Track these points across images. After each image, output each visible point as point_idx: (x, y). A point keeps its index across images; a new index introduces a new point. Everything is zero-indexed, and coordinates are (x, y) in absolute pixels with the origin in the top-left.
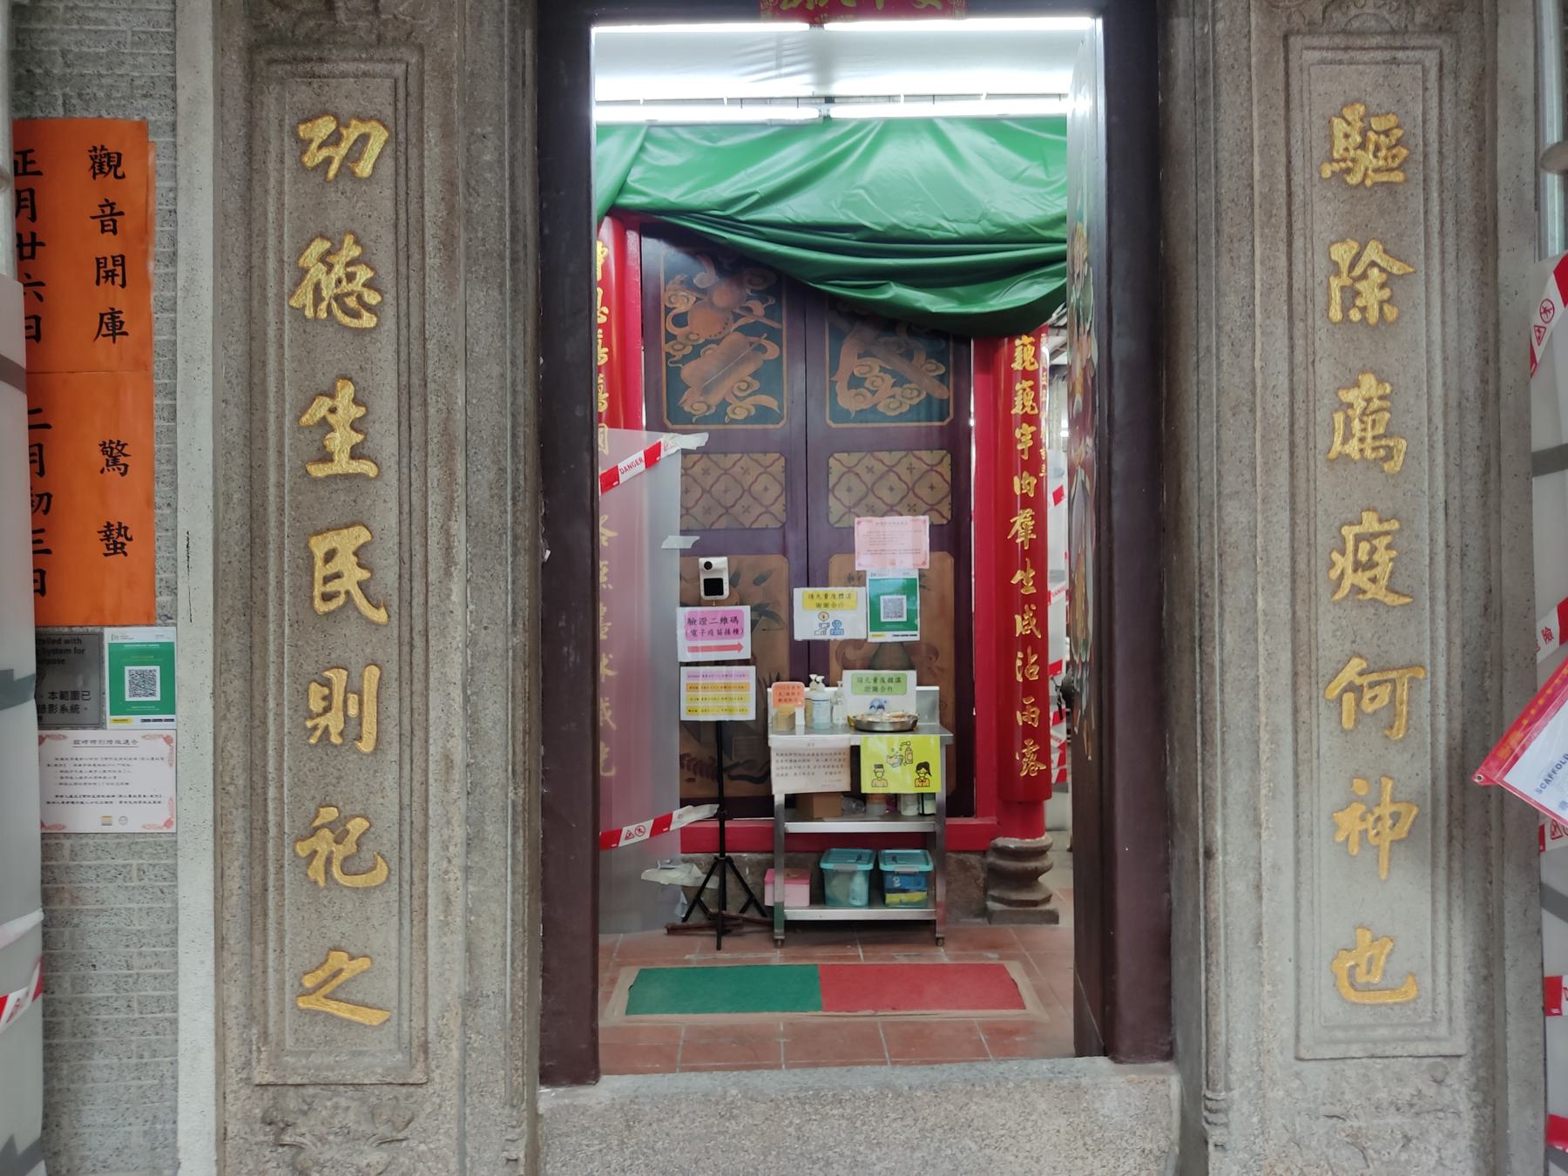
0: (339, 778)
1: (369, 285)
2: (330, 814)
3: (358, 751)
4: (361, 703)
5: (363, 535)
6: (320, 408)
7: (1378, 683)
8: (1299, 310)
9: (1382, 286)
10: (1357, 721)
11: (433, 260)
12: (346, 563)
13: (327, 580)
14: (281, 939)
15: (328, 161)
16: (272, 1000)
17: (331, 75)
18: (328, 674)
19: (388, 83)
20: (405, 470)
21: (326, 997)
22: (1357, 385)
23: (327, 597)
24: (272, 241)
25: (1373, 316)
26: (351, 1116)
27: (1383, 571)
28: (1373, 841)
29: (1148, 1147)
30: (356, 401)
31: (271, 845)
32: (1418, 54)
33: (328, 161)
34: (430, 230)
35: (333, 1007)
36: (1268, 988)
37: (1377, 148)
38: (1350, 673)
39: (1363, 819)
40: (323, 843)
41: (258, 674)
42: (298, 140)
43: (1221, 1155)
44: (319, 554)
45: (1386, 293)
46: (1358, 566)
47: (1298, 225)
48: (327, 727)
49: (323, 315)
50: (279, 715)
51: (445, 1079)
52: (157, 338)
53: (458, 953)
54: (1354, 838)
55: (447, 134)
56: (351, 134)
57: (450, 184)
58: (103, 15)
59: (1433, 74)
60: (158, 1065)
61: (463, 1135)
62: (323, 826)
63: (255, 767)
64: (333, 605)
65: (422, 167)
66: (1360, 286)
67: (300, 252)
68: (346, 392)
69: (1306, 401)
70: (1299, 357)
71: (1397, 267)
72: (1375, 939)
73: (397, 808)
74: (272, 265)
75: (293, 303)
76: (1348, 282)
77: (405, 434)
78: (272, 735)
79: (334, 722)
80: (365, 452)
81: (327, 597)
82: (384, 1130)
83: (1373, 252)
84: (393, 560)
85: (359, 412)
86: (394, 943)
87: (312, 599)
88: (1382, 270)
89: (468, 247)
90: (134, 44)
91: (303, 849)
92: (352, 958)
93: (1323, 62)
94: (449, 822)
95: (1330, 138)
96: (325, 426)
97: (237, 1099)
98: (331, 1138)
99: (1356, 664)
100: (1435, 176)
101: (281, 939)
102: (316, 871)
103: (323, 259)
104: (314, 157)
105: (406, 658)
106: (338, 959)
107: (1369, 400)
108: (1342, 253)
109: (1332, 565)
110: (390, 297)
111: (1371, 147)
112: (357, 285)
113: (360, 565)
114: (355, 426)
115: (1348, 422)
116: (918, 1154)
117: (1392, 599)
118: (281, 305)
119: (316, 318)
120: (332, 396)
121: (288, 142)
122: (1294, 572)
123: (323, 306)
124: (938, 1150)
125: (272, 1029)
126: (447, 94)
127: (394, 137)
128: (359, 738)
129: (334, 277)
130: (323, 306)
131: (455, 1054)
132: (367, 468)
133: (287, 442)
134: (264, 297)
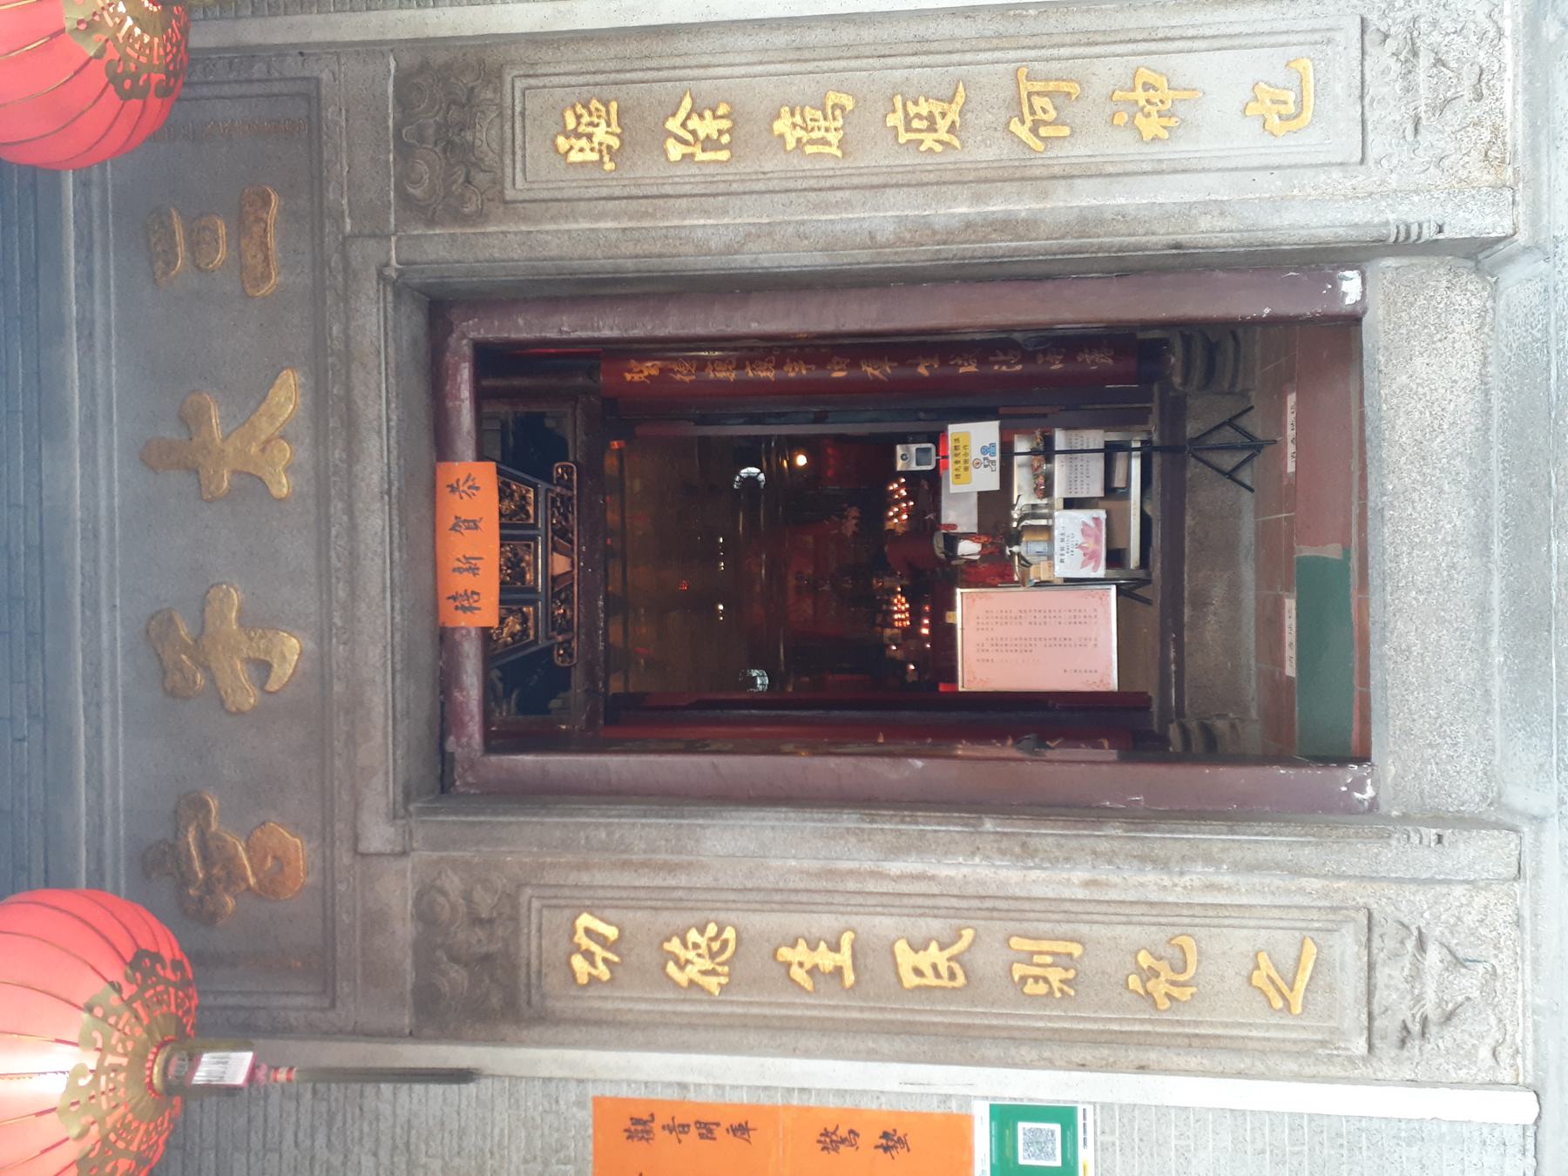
0: (1103, 973)
1: (702, 931)
2: (1134, 982)
3: (1081, 957)
4: (1040, 953)
5: (901, 947)
6: (798, 974)
7: (1031, 106)
8: (722, 188)
9: (701, 116)
10: (1064, 124)
11: (683, 880)
12: (924, 960)
13: (938, 975)
14: (1241, 1025)
15: (605, 961)
16: (1294, 1035)
17: (540, 957)
18: (1016, 978)
19: (545, 912)
20: (849, 909)
21: (1292, 990)
22: (782, 136)
23: (952, 976)
24: (668, 1007)
25: (725, 124)
26: (1396, 973)
27: (937, 108)
28: (1168, 105)
29: (1445, 284)
30: (794, 945)
31: (1159, 1029)
32: (518, 94)
33: (605, 961)
34: (658, 882)
35: (1301, 985)
36: (1296, 192)
37: (591, 124)
38: (1022, 132)
39: (1148, 115)
40: (1159, 988)
41: (1017, 1034)
42: (589, 984)
43: (1446, 228)
44: (917, 981)
45: (708, 114)
46: (932, 128)
47: (654, 191)
48: (1061, 981)
49: (726, 969)
50: (1050, 1018)
51: (1363, 895)
52: (745, 1101)
53: (1255, 879)
54: (1164, 121)
55: (585, 866)
56: (585, 943)
57: (625, 865)
58: (497, 1131)
59: (532, 82)
60: (1349, 1133)
61: (1414, 880)
62: (1144, 987)
63: (1095, 1039)
65: (612, 887)
66: (702, 135)
67: (676, 985)
68: (785, 953)
69: (796, 179)
70: (760, 186)
71: (687, 103)
72: (1256, 99)
73: (1131, 928)
74: (687, 1008)
75: (717, 993)
76: (699, 146)
78: (1067, 1025)
79: (1055, 975)
80: (834, 940)
81: (952, 976)
82: (1411, 945)
83: (673, 125)
84: (921, 922)
85: (802, 945)
86: (1245, 932)
87: (954, 988)
88: (688, 117)
89: (672, 853)
90: (518, 1108)
91: (1164, 1004)
92: (1257, 967)
93: (524, 171)
94: (1142, 885)
95: (583, 164)
96: (813, 971)
97: (1381, 1070)
98: (1416, 992)
99: (1015, 126)
100: (613, 76)
101: (1241, 1025)
102: (1184, 994)
103: (682, 965)
104: (603, 972)
105: (1002, 915)
106: (1259, 979)
107: (794, 125)
108: (675, 151)
109: (930, 150)
110: (712, 915)
111: (590, 129)
113: (926, 948)
114: (813, 947)
115: (812, 142)
116: (1446, 488)
117: (960, 99)
118: (719, 1002)
119: (729, 975)
120: (788, 965)
121: (591, 992)
122: (937, 183)
123: (719, 969)
124: (1442, 470)
125: (1319, 1037)
126: (553, 866)
127: (590, 910)
128: (1070, 955)
129: (696, 959)
130: (719, 969)
131: (1342, 884)
133: (826, 1002)
134: (712, 1015)
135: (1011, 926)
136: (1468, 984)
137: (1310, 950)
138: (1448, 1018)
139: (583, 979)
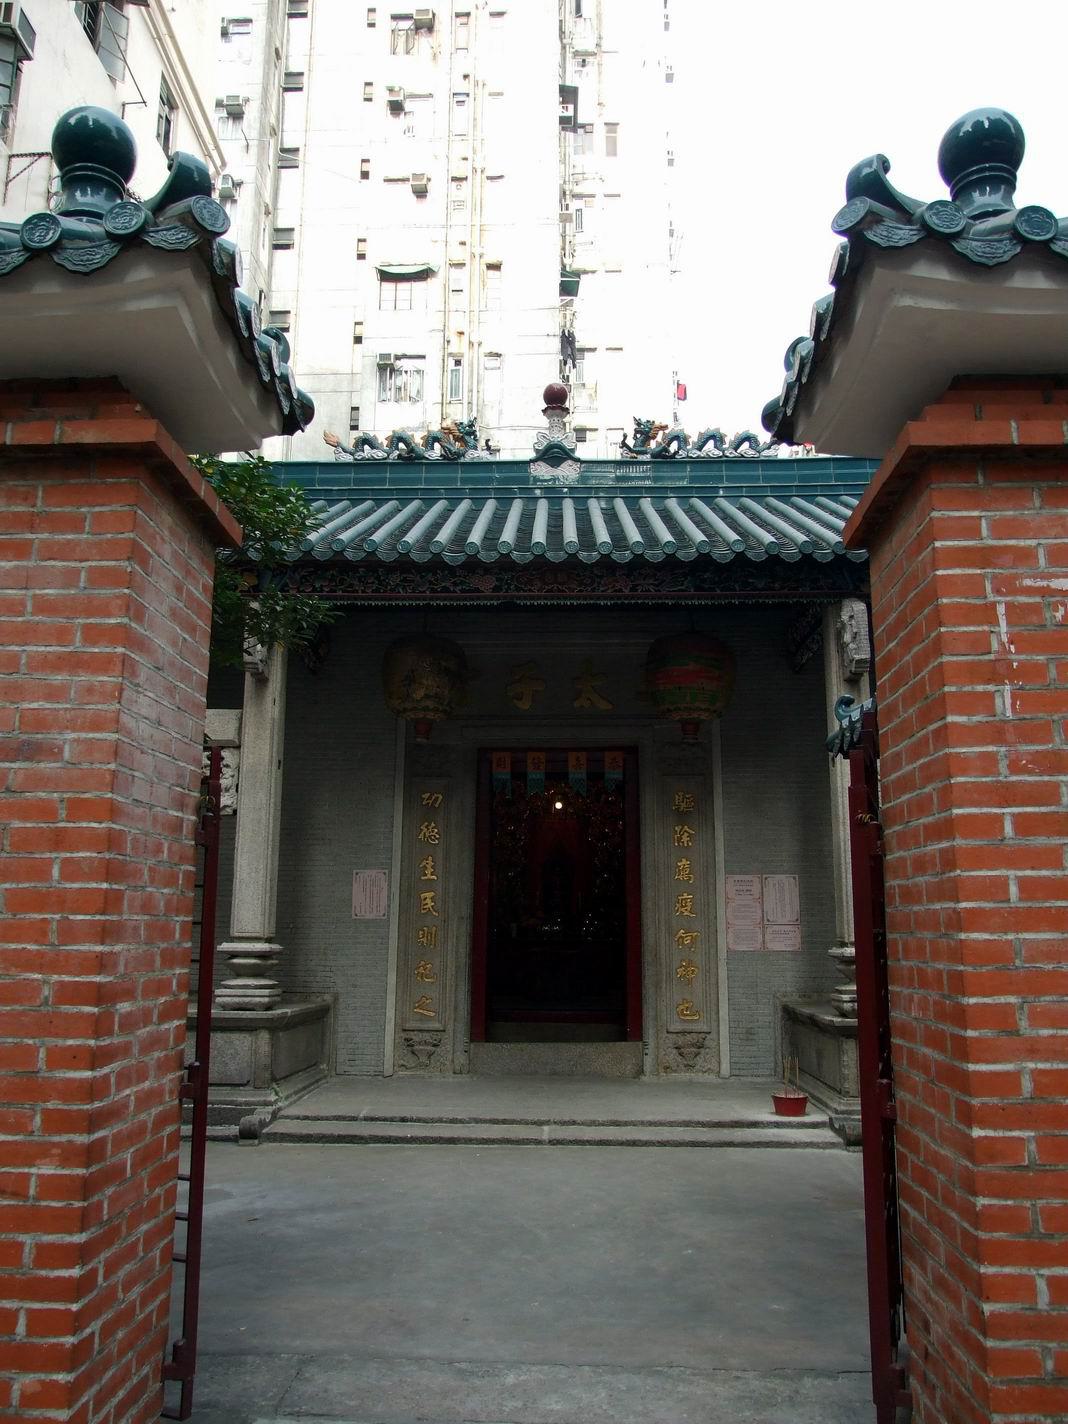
12: (428, 901)
46: (682, 907)
96: (425, 867)
136: (423, 1059)
137: (432, 1014)
138: (413, 1053)
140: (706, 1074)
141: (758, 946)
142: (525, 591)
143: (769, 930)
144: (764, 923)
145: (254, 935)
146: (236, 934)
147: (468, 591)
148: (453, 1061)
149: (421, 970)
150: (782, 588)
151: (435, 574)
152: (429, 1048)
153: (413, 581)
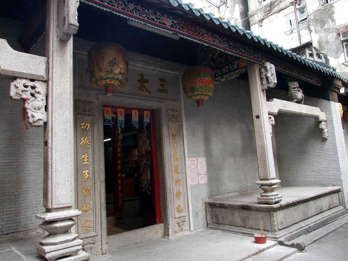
2: (85, 205)
5: (87, 171)
15: (84, 128)
17: (85, 118)
64: (85, 179)
77: (93, 159)
81: (85, 178)
82: (94, 242)
96: (84, 158)
103: (84, 139)
104: (82, 127)
112: (87, 142)
120: (85, 155)
132: (88, 163)
135: (92, 187)
139: (81, 124)
140: (186, 231)
141: (197, 182)
142: (182, 31)
143: (200, 177)
144: (198, 174)
145: (67, 205)
146: (55, 207)
147: (162, 23)
148: (102, 249)
149: (85, 208)
150: (248, 55)
151: (148, 10)
152: (92, 245)
153: (139, 10)
